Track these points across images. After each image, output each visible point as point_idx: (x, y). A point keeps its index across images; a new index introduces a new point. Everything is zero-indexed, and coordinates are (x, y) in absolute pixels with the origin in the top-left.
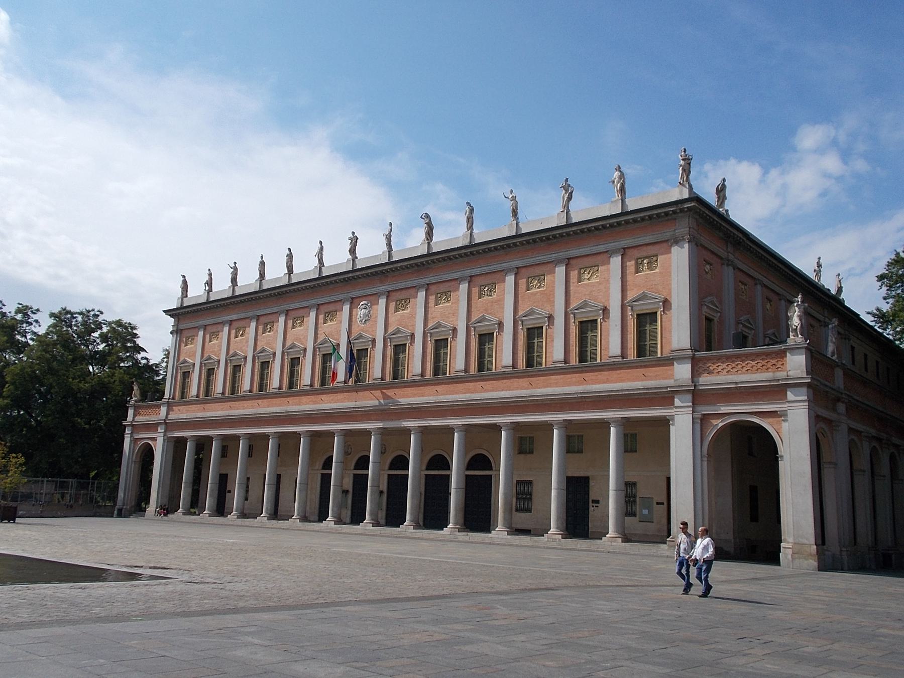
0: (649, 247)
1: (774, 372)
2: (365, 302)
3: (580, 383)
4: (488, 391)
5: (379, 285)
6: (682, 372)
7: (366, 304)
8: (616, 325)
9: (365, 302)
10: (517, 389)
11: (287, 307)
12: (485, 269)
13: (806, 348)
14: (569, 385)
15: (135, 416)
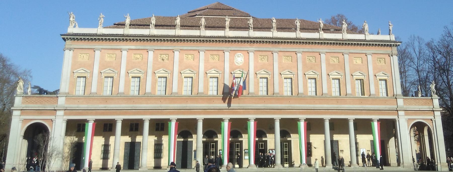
0: (382, 55)
1: (429, 106)
2: (241, 54)
3: (360, 104)
4: (316, 104)
5: (249, 47)
6: (401, 102)
7: (241, 55)
8: (372, 83)
9: (241, 54)
10: (332, 104)
11: (182, 48)
12: (311, 50)
13: (438, 99)
14: (356, 104)
15: (23, 103)
